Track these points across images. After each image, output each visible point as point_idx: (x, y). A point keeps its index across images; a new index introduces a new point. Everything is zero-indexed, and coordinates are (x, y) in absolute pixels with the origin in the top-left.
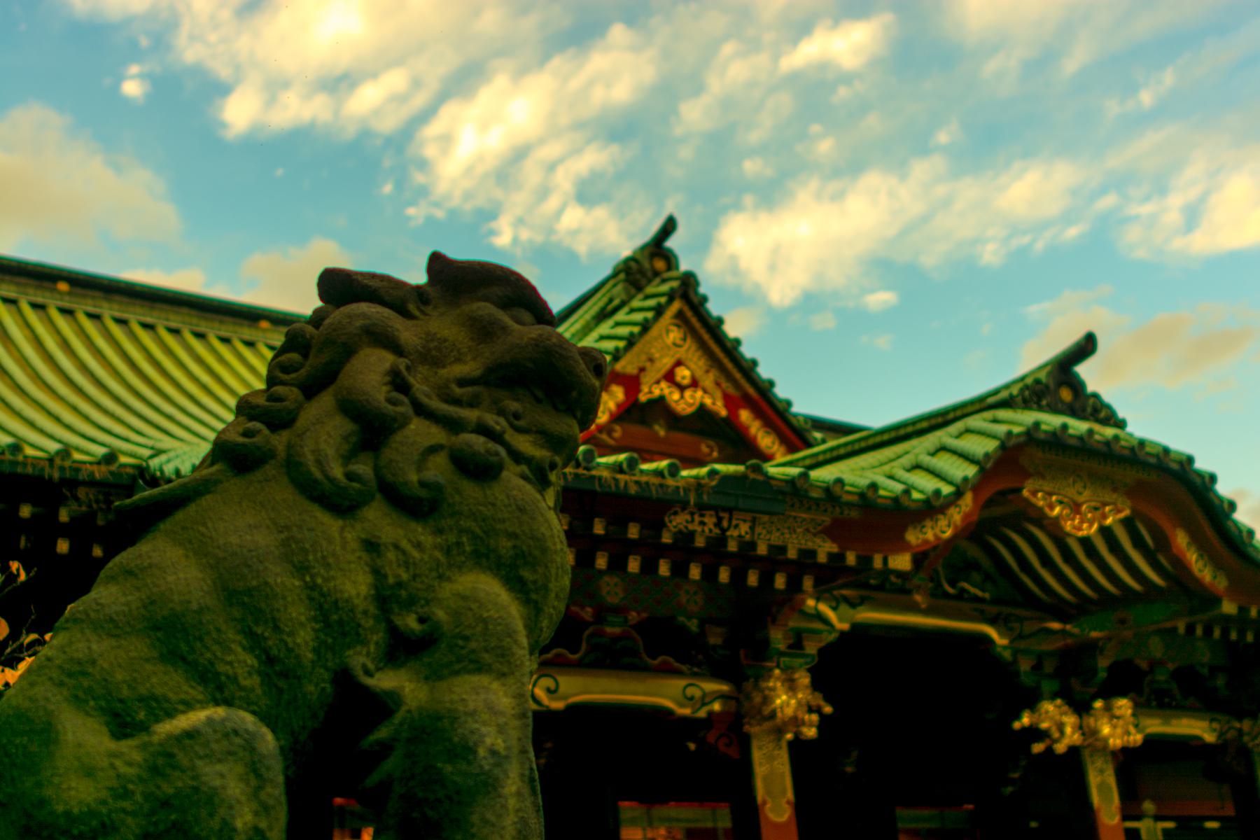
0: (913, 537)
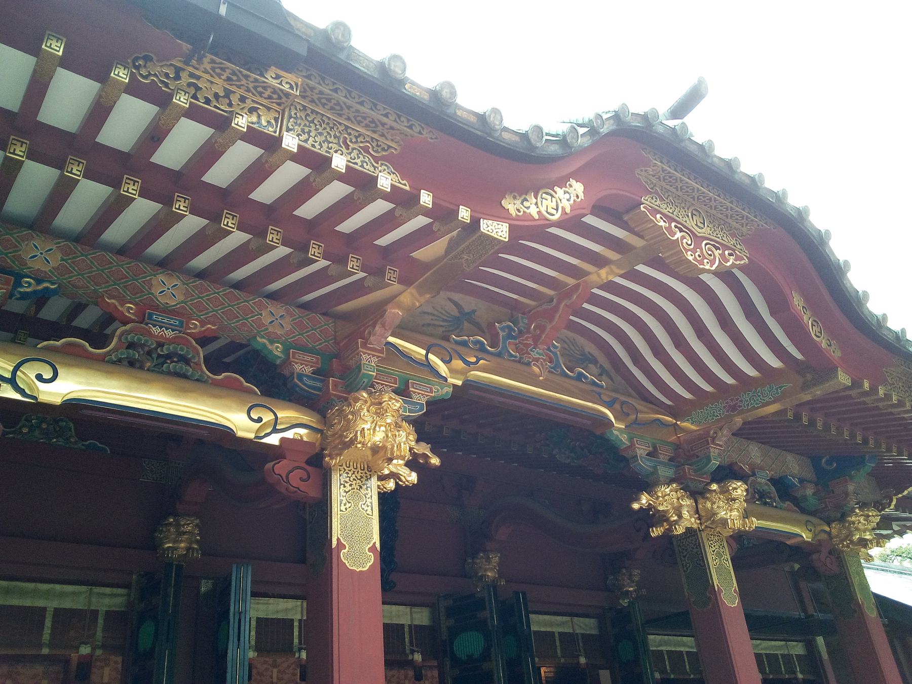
0: (511, 206)
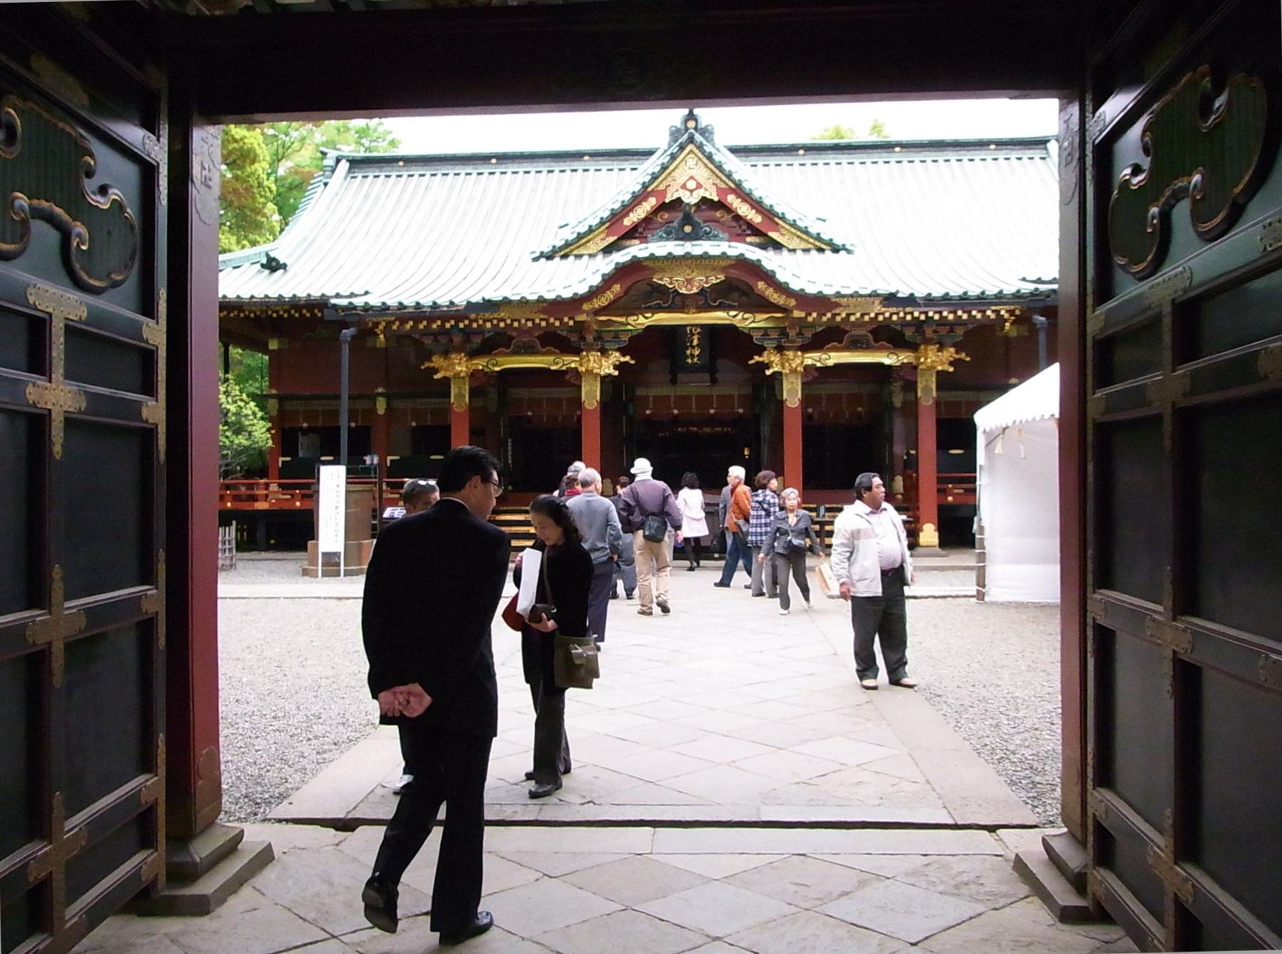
0: (586, 307)
